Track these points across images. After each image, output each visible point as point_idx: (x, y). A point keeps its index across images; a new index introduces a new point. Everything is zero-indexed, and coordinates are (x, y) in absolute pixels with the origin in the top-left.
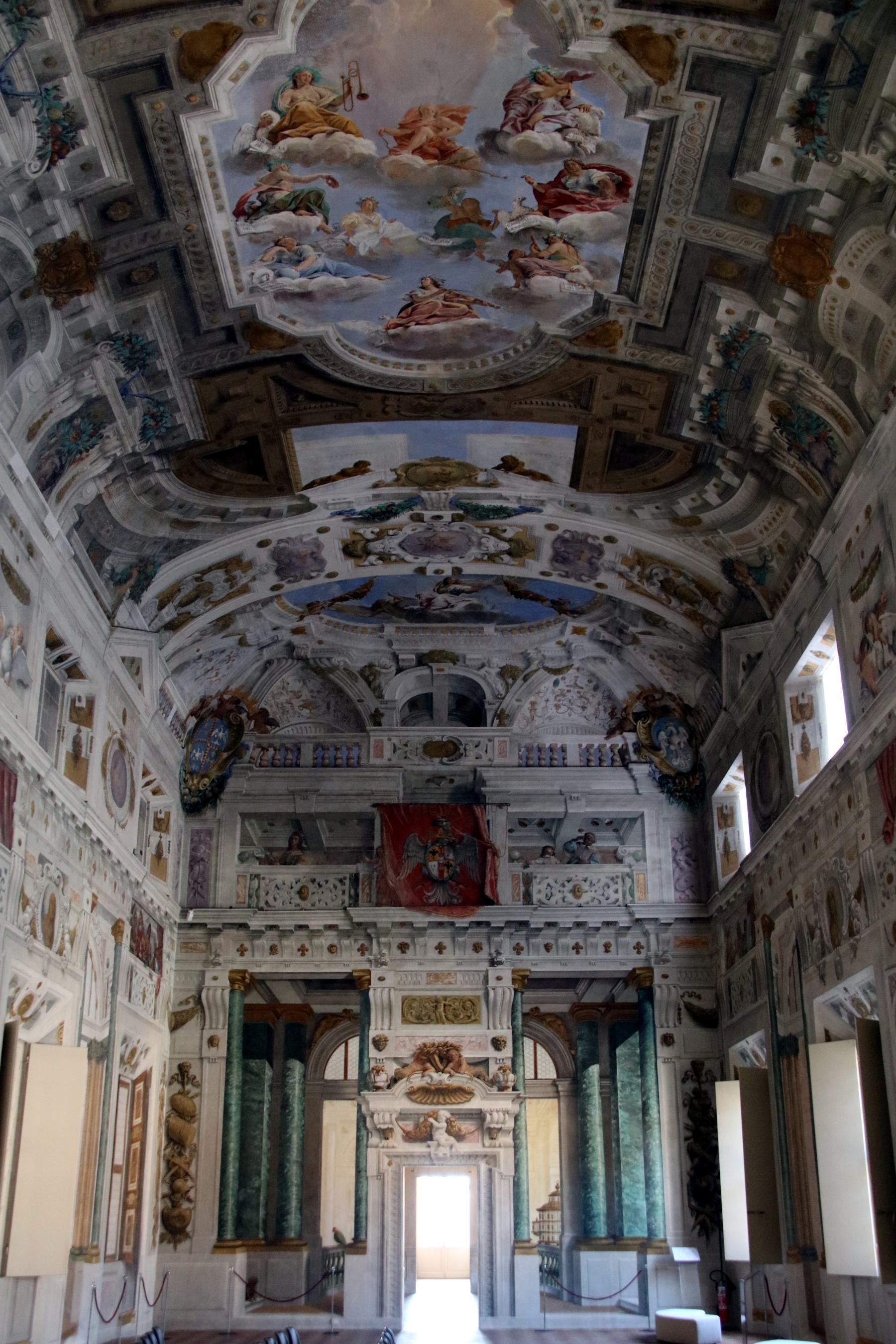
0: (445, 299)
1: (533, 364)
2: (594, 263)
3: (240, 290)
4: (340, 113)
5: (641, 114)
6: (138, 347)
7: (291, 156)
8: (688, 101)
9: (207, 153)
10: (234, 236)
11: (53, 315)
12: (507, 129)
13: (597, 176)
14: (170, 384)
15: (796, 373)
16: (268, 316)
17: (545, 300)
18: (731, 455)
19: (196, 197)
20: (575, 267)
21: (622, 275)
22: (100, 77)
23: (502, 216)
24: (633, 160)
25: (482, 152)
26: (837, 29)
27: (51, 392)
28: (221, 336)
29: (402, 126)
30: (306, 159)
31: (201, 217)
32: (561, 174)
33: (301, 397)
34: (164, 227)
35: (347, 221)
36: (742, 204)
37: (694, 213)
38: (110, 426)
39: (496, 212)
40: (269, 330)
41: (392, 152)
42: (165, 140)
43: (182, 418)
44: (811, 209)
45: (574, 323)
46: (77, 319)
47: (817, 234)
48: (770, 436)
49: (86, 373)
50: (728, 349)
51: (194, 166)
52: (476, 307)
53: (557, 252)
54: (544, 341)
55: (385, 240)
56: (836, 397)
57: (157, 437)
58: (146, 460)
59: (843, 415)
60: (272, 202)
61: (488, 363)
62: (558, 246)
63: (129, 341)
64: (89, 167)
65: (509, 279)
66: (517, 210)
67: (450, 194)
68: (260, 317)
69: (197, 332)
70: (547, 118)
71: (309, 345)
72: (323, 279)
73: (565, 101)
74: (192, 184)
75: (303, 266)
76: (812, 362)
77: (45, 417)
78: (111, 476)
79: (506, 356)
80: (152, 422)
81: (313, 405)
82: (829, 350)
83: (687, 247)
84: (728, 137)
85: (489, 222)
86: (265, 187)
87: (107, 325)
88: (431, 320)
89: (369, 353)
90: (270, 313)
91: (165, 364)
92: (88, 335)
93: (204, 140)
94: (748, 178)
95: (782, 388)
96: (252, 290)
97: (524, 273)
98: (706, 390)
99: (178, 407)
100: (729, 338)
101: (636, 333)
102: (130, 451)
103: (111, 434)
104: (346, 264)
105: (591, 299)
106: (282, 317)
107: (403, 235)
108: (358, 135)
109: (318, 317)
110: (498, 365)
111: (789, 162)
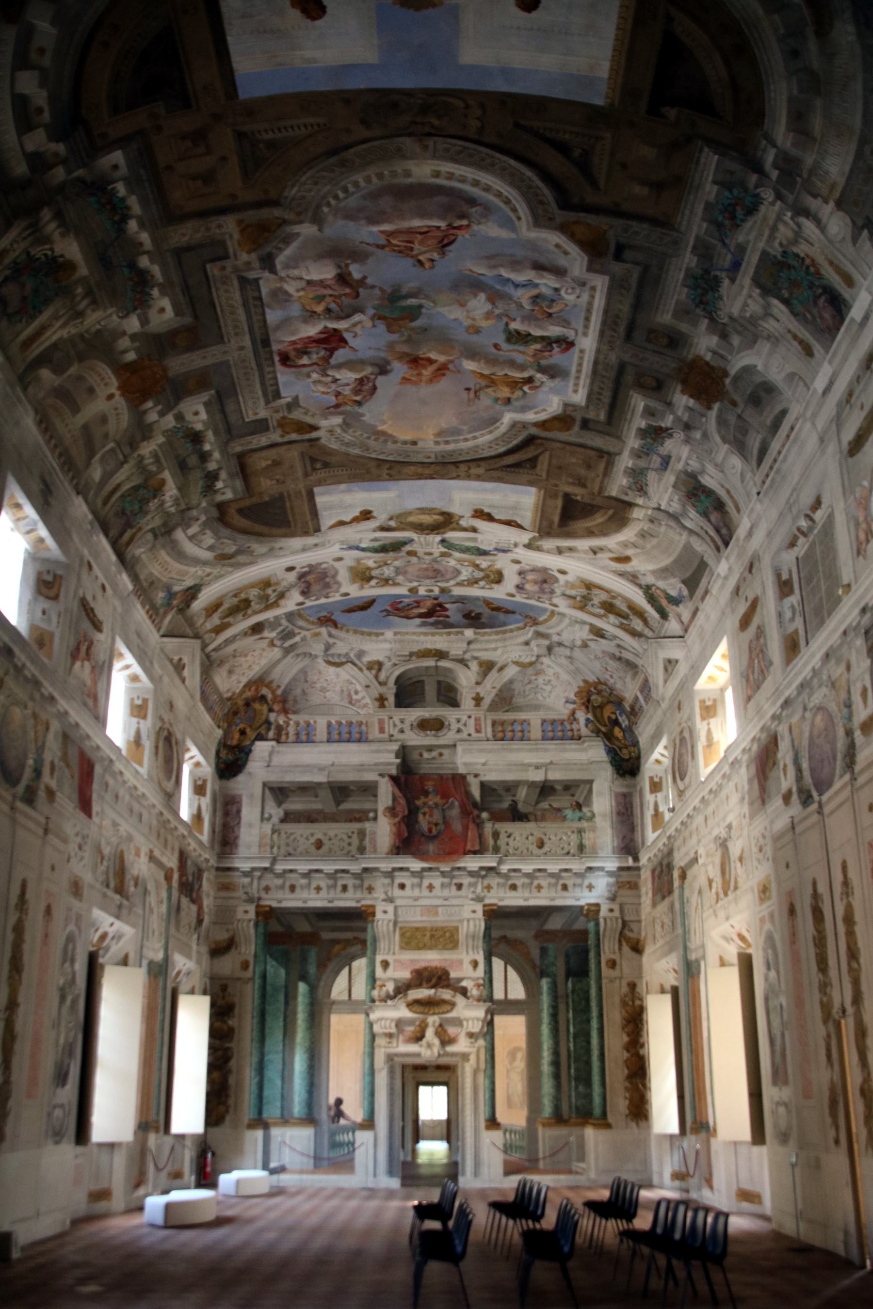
0: (412, 249)
1: (316, 183)
2: (287, 301)
3: (593, 289)
4: (483, 383)
5: (289, 399)
6: (699, 291)
7: (522, 368)
8: (263, 413)
9: (576, 385)
10: (580, 330)
11: (733, 372)
12: (373, 377)
13: (305, 360)
14: (697, 238)
15: (80, 315)
16: (578, 258)
17: (320, 257)
18: (59, 174)
19: (596, 363)
20: (302, 293)
21: (260, 299)
22: (619, 438)
23: (369, 324)
24: (284, 376)
25: (388, 363)
26: (204, 469)
27: (777, 340)
28: (628, 254)
29: (444, 375)
30: (512, 364)
31: (598, 351)
32: (331, 356)
33: (577, 153)
34: (626, 357)
35: (490, 322)
36: (200, 381)
37: (228, 361)
38: (770, 250)
39: (374, 326)
40: (582, 244)
41: (452, 362)
42: (599, 400)
43: (710, 191)
44: (160, 407)
45: (287, 240)
46: (721, 352)
47: (145, 401)
48: (47, 240)
49: (748, 315)
50: (142, 280)
51: (588, 381)
52: (383, 242)
53: (319, 303)
54: (310, 214)
55: (463, 305)
56: (48, 343)
57: (746, 190)
58: (775, 174)
59: (35, 345)
60: (544, 344)
61: (362, 180)
62: (320, 309)
63: (701, 302)
64: (649, 412)
65: (356, 271)
66: (358, 330)
67: (410, 336)
68: (586, 258)
69: (646, 269)
70: (348, 385)
71: (550, 219)
72: (520, 278)
73: (338, 394)
74: (595, 372)
75: (535, 292)
76: (81, 336)
77: (795, 337)
78: (813, 204)
79: (345, 190)
80: (740, 213)
81: (567, 136)
82: (81, 358)
83: (221, 339)
84: (230, 407)
85: (379, 318)
86: (546, 354)
87: (707, 328)
88: (426, 229)
89: (491, 197)
90: (576, 260)
91: (688, 260)
92: (724, 336)
93: (576, 391)
94: (205, 396)
95: (80, 290)
96: (583, 284)
97: (343, 278)
98: (133, 225)
99: (705, 209)
100: (148, 290)
101: (226, 249)
102: (779, 203)
103: (776, 244)
104: (498, 287)
105: (279, 266)
106: (566, 253)
107: (447, 308)
108: (474, 372)
109: (532, 245)
110: (354, 178)
111: (189, 417)
